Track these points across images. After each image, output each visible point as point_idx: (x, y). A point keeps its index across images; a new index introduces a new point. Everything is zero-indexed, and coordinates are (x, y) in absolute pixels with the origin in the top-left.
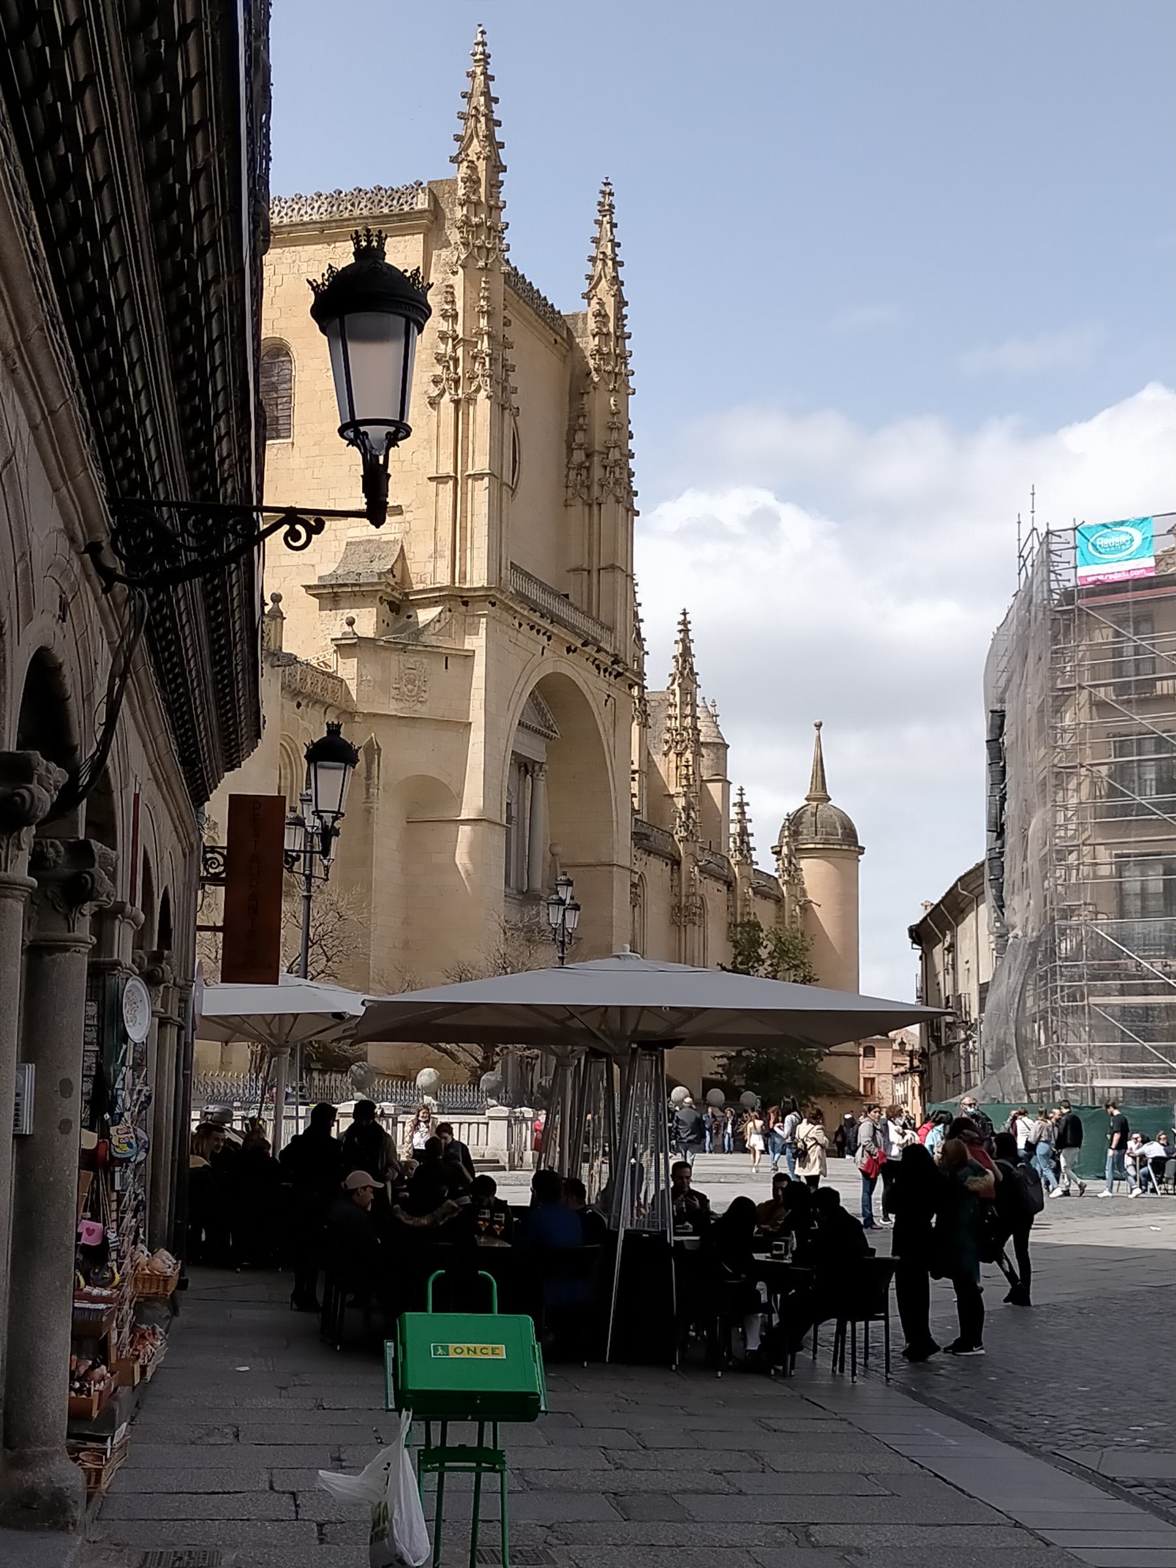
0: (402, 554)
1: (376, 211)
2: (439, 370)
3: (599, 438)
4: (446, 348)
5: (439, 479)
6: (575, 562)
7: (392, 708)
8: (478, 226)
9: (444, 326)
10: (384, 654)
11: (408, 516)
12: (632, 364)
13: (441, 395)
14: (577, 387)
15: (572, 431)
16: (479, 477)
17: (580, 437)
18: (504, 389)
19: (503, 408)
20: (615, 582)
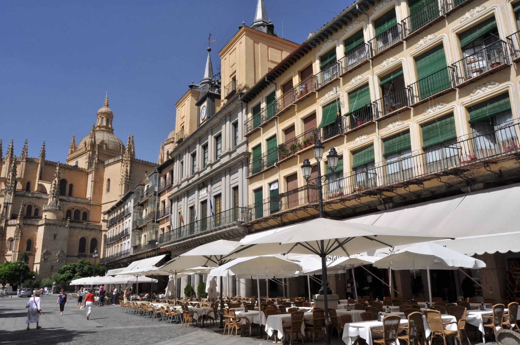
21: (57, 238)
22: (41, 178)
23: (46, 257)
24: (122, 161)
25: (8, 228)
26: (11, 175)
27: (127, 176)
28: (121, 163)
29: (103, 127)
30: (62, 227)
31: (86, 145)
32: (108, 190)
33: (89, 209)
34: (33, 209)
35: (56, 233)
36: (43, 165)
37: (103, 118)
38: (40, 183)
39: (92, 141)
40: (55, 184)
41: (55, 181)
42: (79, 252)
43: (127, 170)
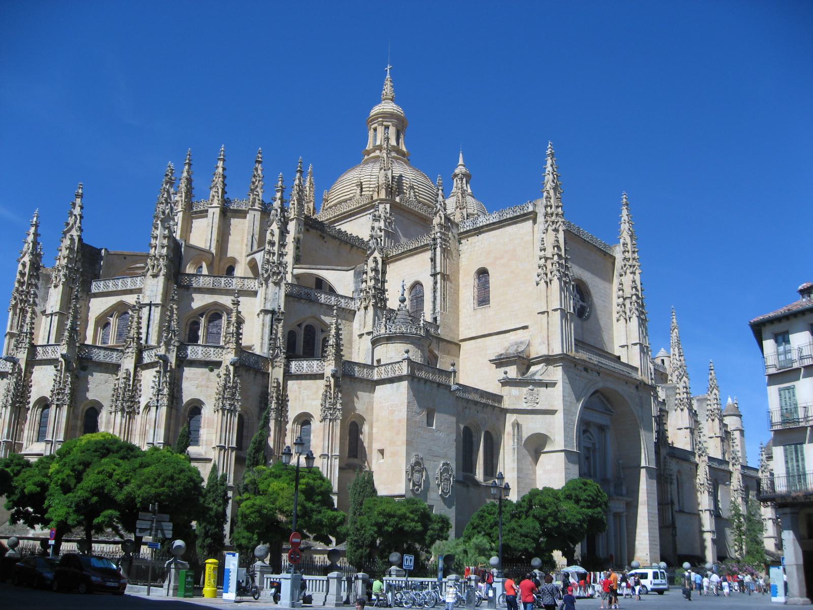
1: (515, 215)
2: (540, 271)
5: (543, 313)
7: (524, 406)
8: (552, 214)
11: (531, 328)
13: (540, 280)
16: (555, 310)
22: (297, 260)
24: (533, 216)
25: (290, 383)
26: (277, 232)
27: (560, 256)
28: (531, 221)
31: (362, 188)
32: (483, 299)
34: (320, 337)
37: (387, 127)
38: (296, 271)
39: (386, 176)
40: (375, 270)
41: (375, 261)
42: (463, 471)
43: (558, 241)
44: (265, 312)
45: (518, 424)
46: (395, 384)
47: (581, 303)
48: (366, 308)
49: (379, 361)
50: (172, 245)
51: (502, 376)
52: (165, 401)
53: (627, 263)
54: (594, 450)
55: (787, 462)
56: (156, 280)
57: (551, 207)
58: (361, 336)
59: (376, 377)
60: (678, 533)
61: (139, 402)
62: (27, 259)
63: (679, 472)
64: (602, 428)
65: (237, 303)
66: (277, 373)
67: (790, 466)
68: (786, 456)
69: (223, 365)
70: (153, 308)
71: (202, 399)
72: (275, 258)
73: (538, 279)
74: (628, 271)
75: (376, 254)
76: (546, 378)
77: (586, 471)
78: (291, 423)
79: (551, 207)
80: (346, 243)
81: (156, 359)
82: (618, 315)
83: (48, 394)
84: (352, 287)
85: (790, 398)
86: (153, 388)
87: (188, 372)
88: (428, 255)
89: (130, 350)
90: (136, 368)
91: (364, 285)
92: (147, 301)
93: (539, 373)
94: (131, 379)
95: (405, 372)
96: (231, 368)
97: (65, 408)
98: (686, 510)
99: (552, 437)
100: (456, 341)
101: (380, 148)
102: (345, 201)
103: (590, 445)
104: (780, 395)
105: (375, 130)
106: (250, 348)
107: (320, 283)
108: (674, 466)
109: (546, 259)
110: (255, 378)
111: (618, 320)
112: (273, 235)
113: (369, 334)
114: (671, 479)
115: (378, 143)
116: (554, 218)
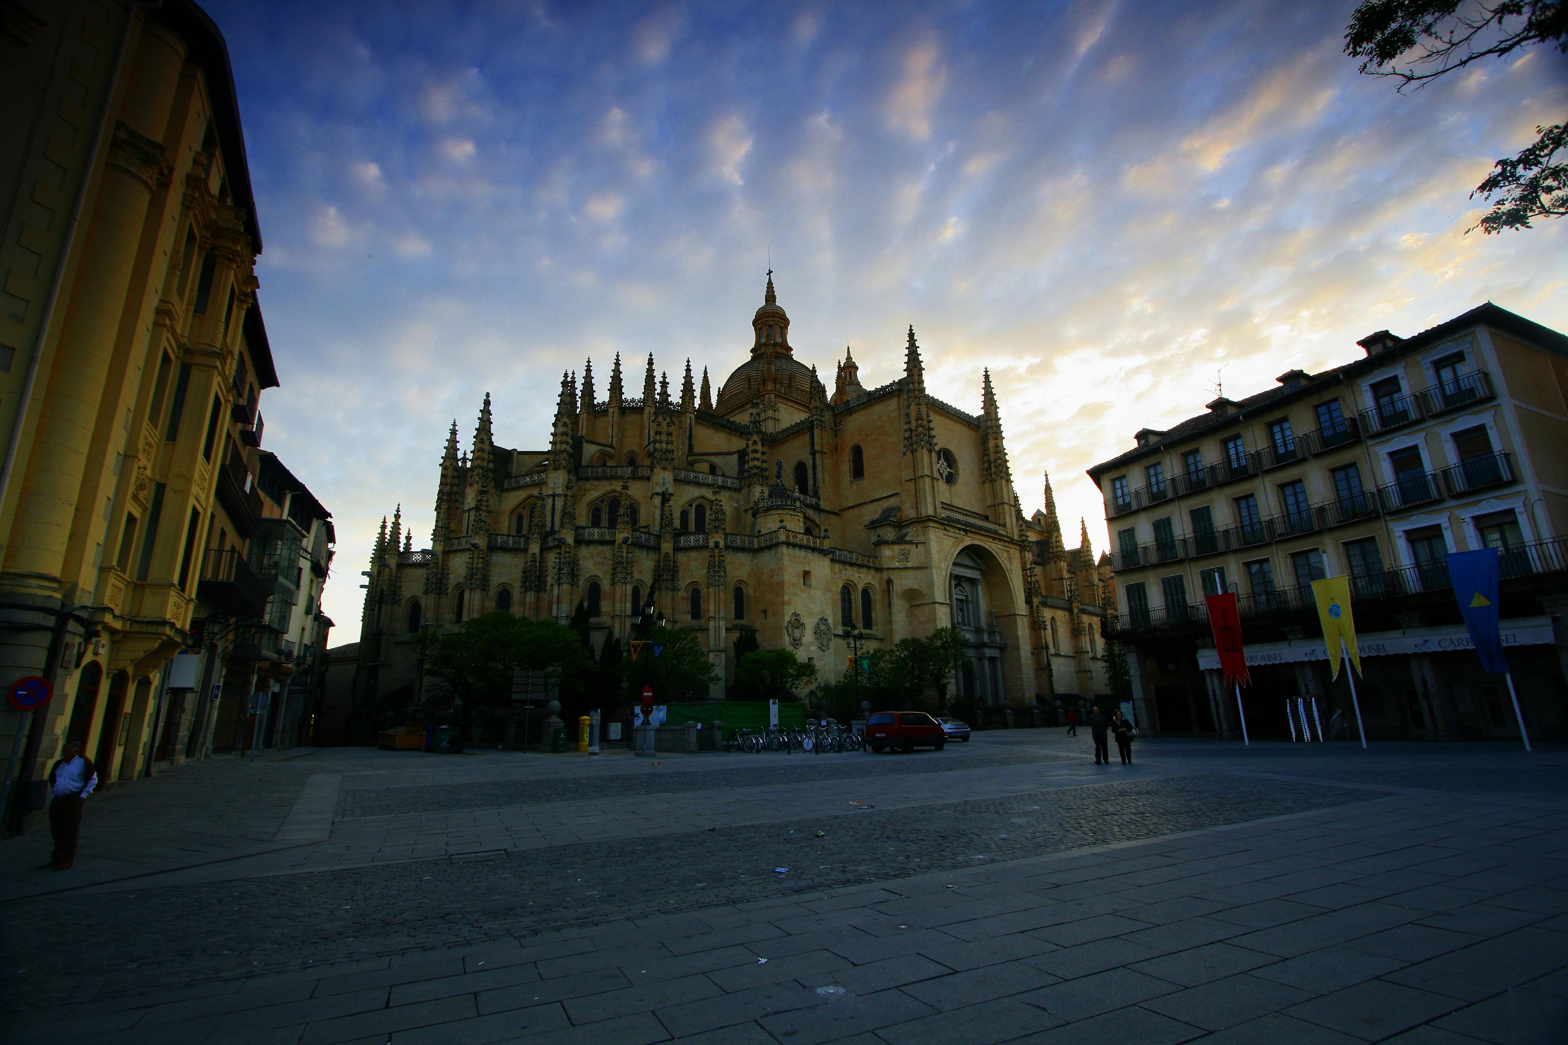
0: (899, 509)
2: (906, 442)
3: (992, 456)
4: (907, 434)
6: (989, 503)
7: (897, 565)
8: (915, 390)
9: (907, 427)
10: (892, 546)
12: (1002, 428)
14: (984, 441)
15: (984, 455)
17: (986, 458)
18: (930, 444)
19: (930, 451)
20: (1004, 509)
21: (814, 582)
23: (797, 633)
29: (775, 345)
30: (816, 554)
32: (858, 472)
33: (818, 521)
35: (807, 569)
36: (693, 416)
38: (690, 458)
41: (755, 443)
42: (844, 625)
44: (657, 494)
45: (892, 582)
46: (773, 552)
47: (949, 470)
48: (749, 486)
49: (759, 531)
50: (571, 442)
51: (874, 539)
52: (564, 579)
53: (990, 431)
54: (967, 602)
55: (1129, 601)
56: (559, 472)
57: (913, 383)
58: (746, 511)
59: (756, 546)
60: (1054, 674)
61: (546, 581)
62: (448, 464)
63: (1053, 618)
64: (973, 582)
65: (625, 487)
66: (667, 547)
67: (1133, 604)
68: (1128, 595)
69: (617, 543)
70: (556, 498)
71: (600, 574)
72: (664, 446)
73: (905, 450)
74: (991, 438)
75: (755, 437)
76: (917, 540)
77: (960, 620)
78: (682, 591)
79: (913, 383)
80: (736, 431)
81: (556, 543)
82: (984, 479)
83: (462, 580)
84: (736, 468)
85: (1129, 540)
86: (554, 568)
87: (584, 551)
88: (807, 438)
89: (536, 536)
90: (542, 551)
91: (746, 466)
92: (550, 492)
93: (910, 534)
94: (538, 559)
95: (780, 541)
96: (625, 547)
97: (478, 591)
98: (1062, 653)
99: (924, 592)
100: (836, 511)
101: (764, 345)
102: (737, 394)
103: (963, 598)
104: (1120, 538)
105: (760, 329)
106: (647, 527)
107: (713, 470)
108: (1047, 614)
109: (911, 431)
110: (648, 554)
111: (984, 483)
112: (659, 425)
113: (752, 508)
114: (1045, 625)
115: (763, 341)
116: (917, 393)
